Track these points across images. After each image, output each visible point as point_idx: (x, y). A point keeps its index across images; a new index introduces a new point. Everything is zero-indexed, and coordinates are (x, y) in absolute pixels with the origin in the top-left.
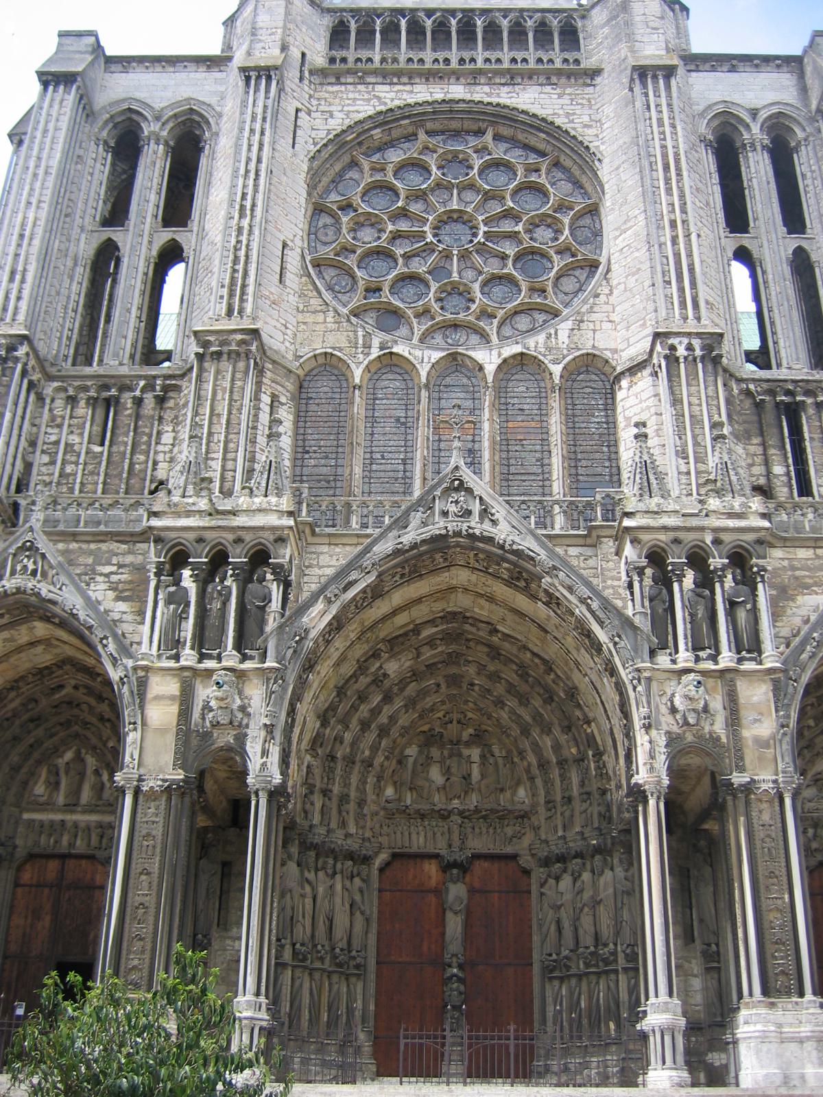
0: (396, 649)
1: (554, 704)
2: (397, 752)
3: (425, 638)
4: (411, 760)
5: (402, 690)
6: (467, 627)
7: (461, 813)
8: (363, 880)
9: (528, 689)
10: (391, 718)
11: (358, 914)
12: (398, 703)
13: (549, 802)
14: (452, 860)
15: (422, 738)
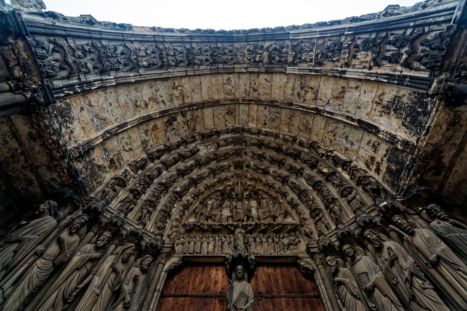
0: (205, 140)
1: (302, 156)
2: (201, 197)
3: (222, 139)
4: (210, 206)
5: (208, 163)
6: (245, 134)
7: (245, 227)
8: (144, 271)
9: (284, 157)
10: (198, 176)
11: (121, 306)
12: (205, 170)
13: (315, 212)
14: (236, 254)
15: (218, 194)
